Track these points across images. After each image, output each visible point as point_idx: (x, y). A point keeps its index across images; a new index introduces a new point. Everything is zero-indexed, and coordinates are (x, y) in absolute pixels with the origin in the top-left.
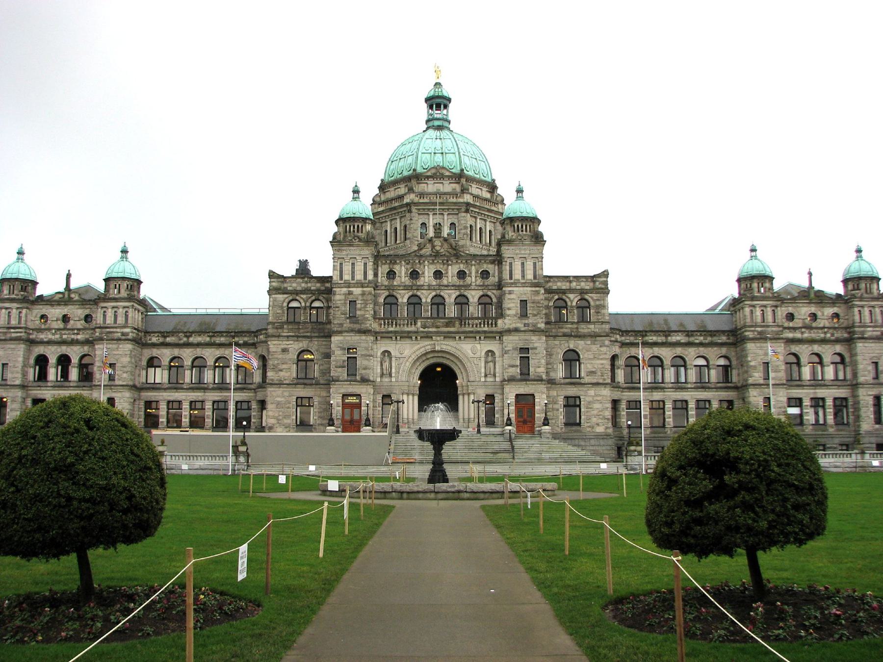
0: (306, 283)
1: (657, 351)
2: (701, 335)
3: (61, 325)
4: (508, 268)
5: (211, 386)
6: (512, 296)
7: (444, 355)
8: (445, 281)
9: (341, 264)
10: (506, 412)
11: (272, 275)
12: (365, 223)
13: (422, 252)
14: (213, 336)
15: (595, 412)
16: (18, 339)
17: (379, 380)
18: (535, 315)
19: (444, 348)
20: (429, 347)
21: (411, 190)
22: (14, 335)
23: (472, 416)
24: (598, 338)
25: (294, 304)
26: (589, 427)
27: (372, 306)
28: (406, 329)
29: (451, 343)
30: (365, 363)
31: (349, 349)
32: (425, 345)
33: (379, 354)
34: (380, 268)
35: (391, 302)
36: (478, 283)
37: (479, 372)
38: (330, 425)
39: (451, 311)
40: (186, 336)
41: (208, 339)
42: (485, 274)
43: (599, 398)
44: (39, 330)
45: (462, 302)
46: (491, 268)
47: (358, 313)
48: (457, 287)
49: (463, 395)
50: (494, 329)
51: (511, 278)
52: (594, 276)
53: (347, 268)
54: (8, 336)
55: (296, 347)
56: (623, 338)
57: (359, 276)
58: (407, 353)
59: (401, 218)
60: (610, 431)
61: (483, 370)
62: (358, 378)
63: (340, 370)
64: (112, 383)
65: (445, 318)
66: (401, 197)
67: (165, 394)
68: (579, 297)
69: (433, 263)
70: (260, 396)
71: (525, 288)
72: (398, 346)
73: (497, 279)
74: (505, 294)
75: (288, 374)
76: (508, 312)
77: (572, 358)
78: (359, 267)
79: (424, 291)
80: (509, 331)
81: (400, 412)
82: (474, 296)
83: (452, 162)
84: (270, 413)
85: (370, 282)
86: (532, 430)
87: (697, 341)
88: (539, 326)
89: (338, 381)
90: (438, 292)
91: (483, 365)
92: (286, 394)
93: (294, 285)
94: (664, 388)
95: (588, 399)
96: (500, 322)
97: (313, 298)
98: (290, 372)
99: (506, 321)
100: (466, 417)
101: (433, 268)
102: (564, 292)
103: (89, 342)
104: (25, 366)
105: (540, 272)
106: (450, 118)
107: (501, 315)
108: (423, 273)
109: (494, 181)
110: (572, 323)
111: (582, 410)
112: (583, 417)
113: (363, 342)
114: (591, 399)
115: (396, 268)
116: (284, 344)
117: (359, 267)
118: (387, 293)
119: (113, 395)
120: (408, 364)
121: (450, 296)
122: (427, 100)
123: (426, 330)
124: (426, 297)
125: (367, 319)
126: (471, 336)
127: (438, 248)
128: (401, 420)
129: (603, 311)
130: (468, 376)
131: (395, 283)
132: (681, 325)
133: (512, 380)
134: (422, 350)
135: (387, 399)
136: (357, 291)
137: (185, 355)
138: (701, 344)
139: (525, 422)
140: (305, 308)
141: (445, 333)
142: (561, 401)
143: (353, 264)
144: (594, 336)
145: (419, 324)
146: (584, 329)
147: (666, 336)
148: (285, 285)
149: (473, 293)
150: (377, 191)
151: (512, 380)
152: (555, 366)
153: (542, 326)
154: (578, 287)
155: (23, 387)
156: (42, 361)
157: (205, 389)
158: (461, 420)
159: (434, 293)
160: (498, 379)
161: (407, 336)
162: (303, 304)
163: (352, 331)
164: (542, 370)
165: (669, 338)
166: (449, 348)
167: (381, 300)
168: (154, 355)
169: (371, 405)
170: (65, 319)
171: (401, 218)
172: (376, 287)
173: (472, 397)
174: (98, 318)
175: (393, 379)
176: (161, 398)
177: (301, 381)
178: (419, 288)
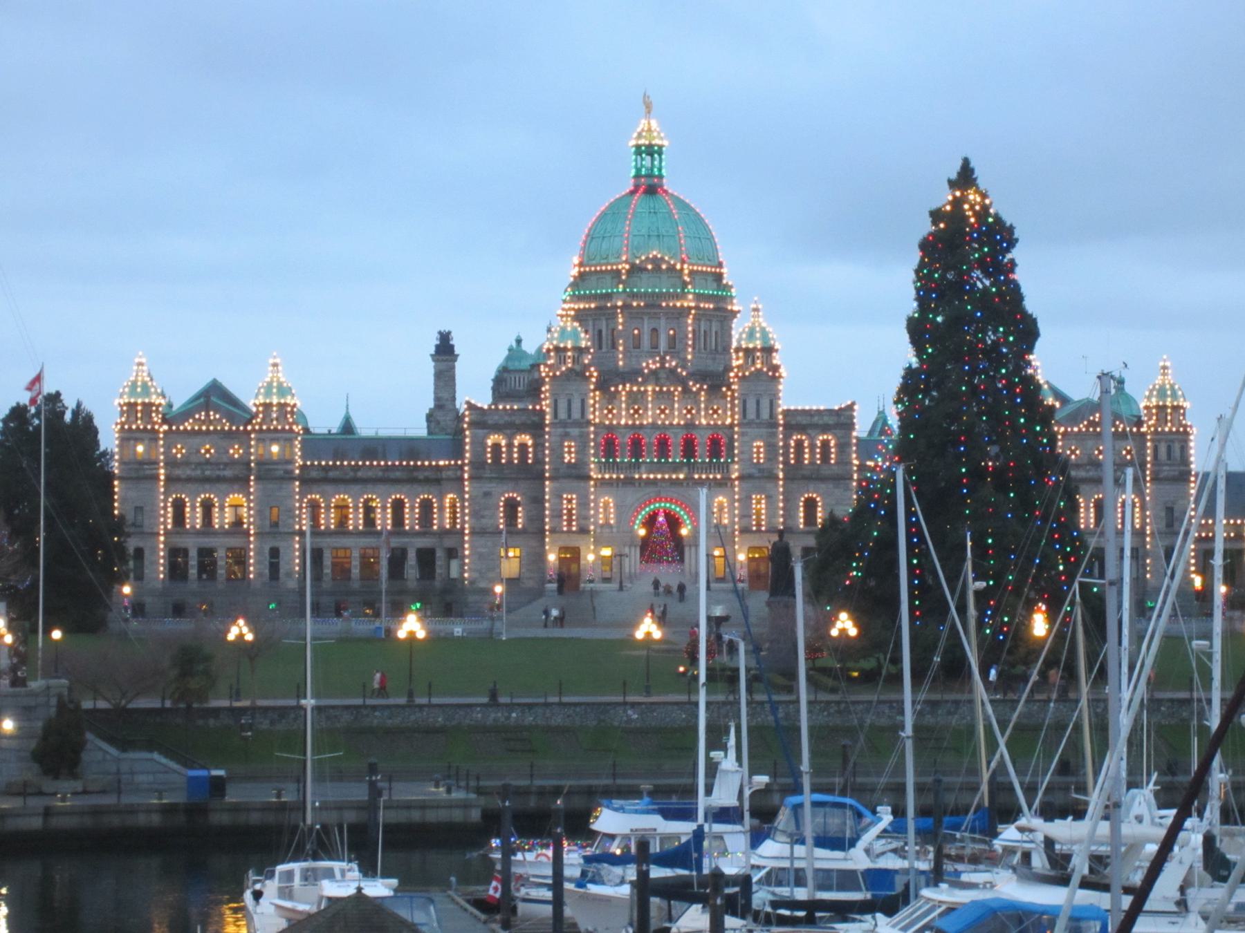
6: (746, 439)
10: (738, 566)
22: (148, 472)
52: (841, 409)
53: (563, 406)
54: (141, 473)
57: (576, 415)
64: (275, 530)
70: (449, 542)
78: (576, 406)
92: (489, 544)
93: (496, 417)
108: (646, 409)
116: (487, 486)
117: (576, 406)
119: (276, 544)
133: (745, 530)
136: (575, 431)
141: (670, 479)
145: (643, 468)
160: (729, 530)
161: (629, 482)
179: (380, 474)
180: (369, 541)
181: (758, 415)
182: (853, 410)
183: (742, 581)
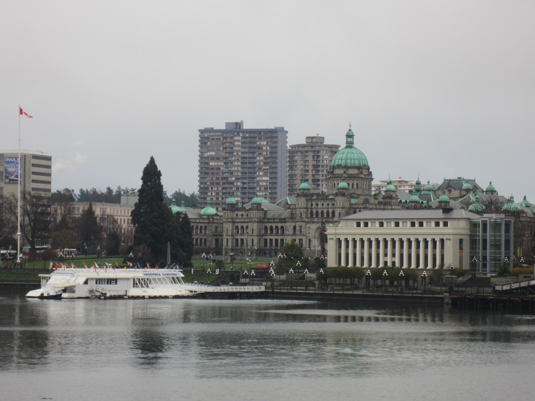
3: (241, 217)
16: (230, 222)
35: (312, 213)
39: (325, 216)
42: (334, 205)
44: (236, 219)
45: (328, 212)
53: (300, 204)
82: (330, 211)
98: (291, 232)
103: (247, 222)
104: (232, 229)
113: (303, 224)
121: (325, 211)
122: (347, 136)
124: (320, 211)
135: (310, 240)
136: (302, 210)
155: (232, 235)
156: (237, 227)
157: (278, 235)
161: (313, 222)
167: (309, 212)
170: (242, 215)
174: (249, 216)
178: (318, 208)
180: (276, 237)
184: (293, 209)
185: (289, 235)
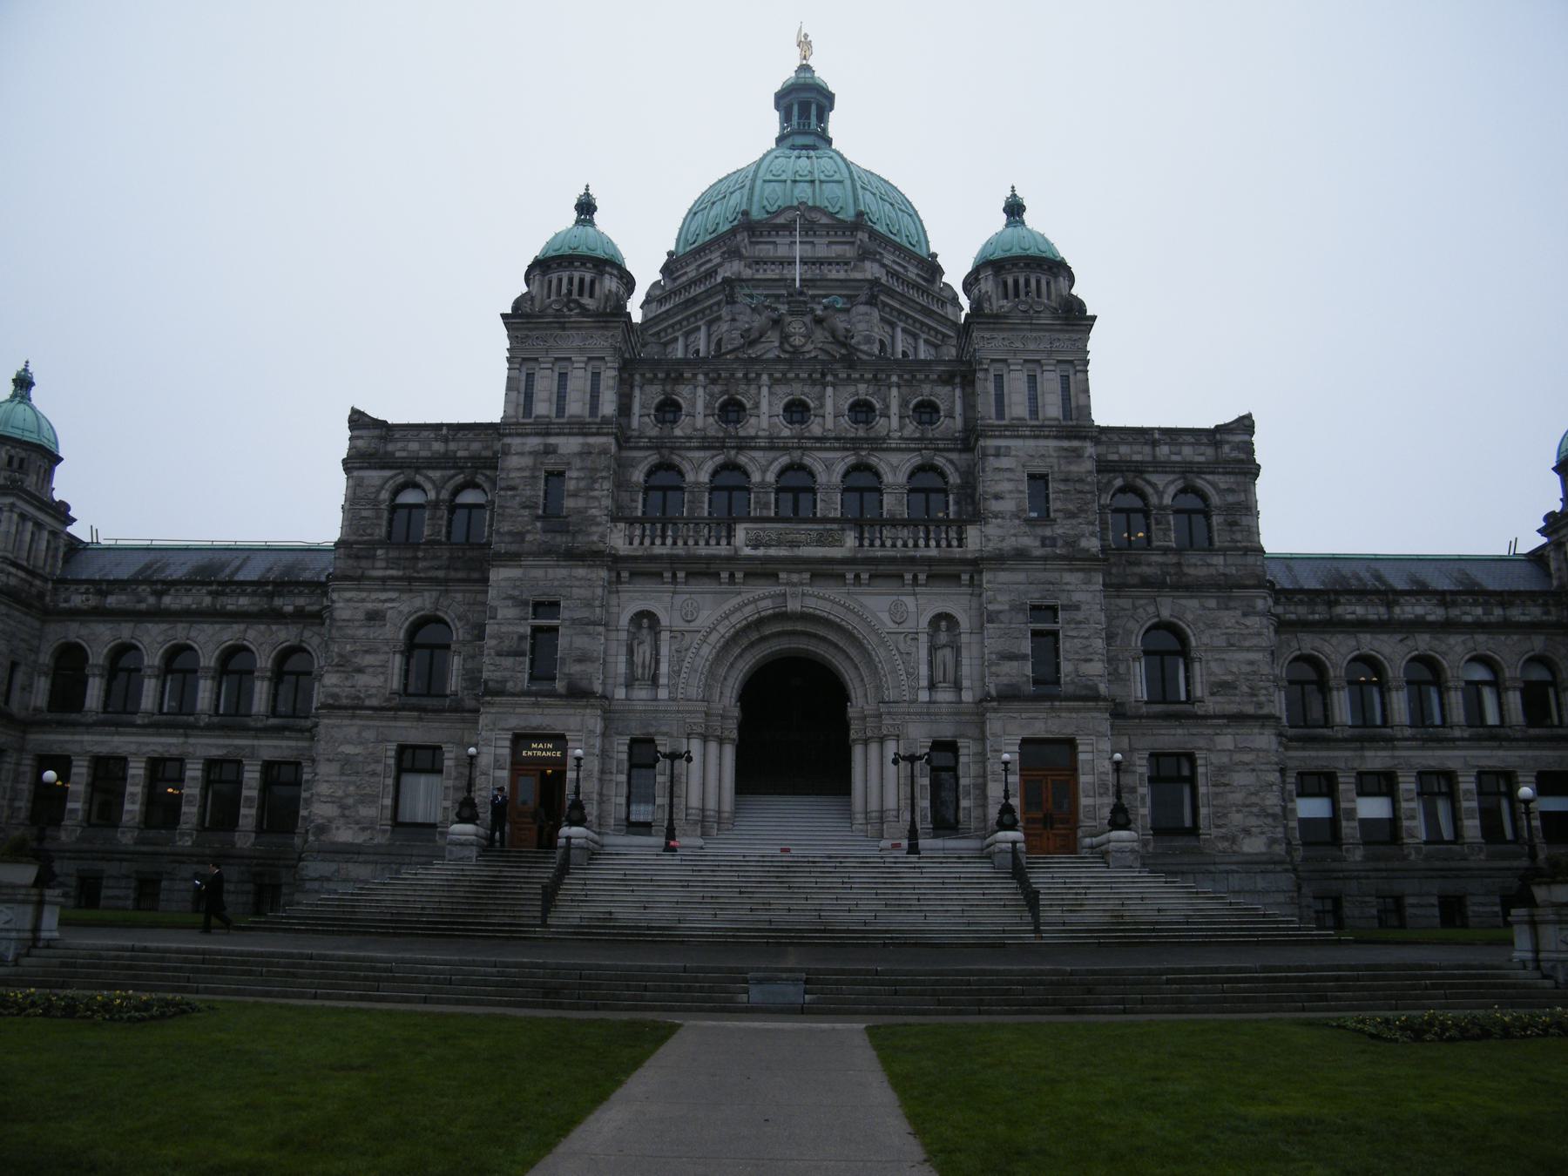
0: (446, 440)
1: (1370, 643)
2: (1475, 604)
4: (991, 387)
5: (205, 720)
6: (1005, 462)
7: (811, 629)
8: (816, 429)
9: (530, 377)
10: (995, 791)
11: (358, 421)
12: (602, 273)
13: (753, 352)
14: (223, 594)
15: (1238, 797)
17: (620, 693)
18: (1071, 515)
19: (814, 605)
20: (768, 603)
21: (735, 254)
23: (891, 803)
24: (1236, 593)
25: (410, 497)
26: (1224, 838)
27: (607, 485)
28: (703, 550)
29: (832, 591)
30: (581, 642)
31: (537, 605)
32: (757, 599)
33: (624, 620)
34: (637, 392)
36: (906, 433)
37: (912, 675)
38: (462, 820)
39: (830, 504)
40: (154, 593)
41: (207, 600)
42: (927, 410)
43: (1247, 758)
45: (862, 482)
46: (949, 398)
47: (569, 503)
48: (852, 444)
49: (866, 742)
50: (957, 552)
51: (1000, 414)
52: (1219, 429)
53: (545, 385)
55: (405, 608)
56: (1279, 610)
58: (705, 618)
59: (710, 324)
60: (1280, 849)
61: (924, 670)
62: (560, 686)
63: (508, 662)
65: (815, 520)
66: (712, 273)
67: (86, 738)
68: (1180, 484)
69: (784, 380)
71: (1042, 442)
72: (679, 599)
73: (959, 423)
74: (985, 455)
75: (378, 681)
76: (995, 506)
77: (1169, 647)
78: (579, 382)
79: (757, 454)
80: (999, 560)
81: (680, 790)
82: (895, 469)
83: (835, 198)
84: (323, 789)
85: (606, 421)
86: (1069, 846)
87: (1468, 619)
88: (1084, 543)
89: (501, 693)
90: (797, 454)
91: (923, 653)
92: (369, 735)
93: (414, 446)
94: (1392, 739)
95: (1215, 759)
96: (972, 534)
97: (460, 478)
98: (383, 674)
99: (992, 529)
100: (874, 805)
101: (784, 395)
102: (1139, 469)
105: (1082, 397)
106: (832, 132)
107: (973, 511)
108: (757, 406)
109: (935, 256)
110: (1166, 551)
111: (1202, 790)
112: (1203, 811)
113: (578, 585)
114: (1225, 760)
115: (683, 394)
116: (375, 600)
117: (579, 382)
118: (653, 458)
120: (705, 650)
121: (829, 469)
123: (761, 552)
124: (763, 469)
125: (593, 521)
126: (886, 572)
127: (797, 341)
128: (680, 815)
129: (1245, 521)
130: (879, 688)
131: (678, 432)
132: (1417, 582)
133: (1009, 696)
134: (748, 610)
136: (569, 445)
137: (146, 640)
138: (1479, 626)
139: (1048, 821)
140: (435, 505)
142: (1142, 767)
143: (563, 377)
144: (1225, 587)
145: (741, 532)
146: (1198, 567)
147: (1389, 606)
148: (390, 447)
149: (894, 458)
150: (659, 277)
151: (1009, 696)
152: (1122, 669)
153: (1093, 544)
154: (1175, 458)
157: (189, 729)
158: (859, 818)
159: (785, 460)
160: (967, 696)
161: (703, 570)
162: (432, 495)
163: (546, 552)
164: (1096, 668)
165: (1397, 610)
166: (828, 606)
167: (638, 476)
168: (72, 638)
169: (593, 765)
171: (710, 324)
172: (624, 440)
173: (891, 748)
175: (663, 694)
176: (76, 748)
177: (414, 700)
178: (744, 445)
179: (207, 600)
181: (1034, 412)
182: (1252, 433)
183: (1012, 828)
184: (416, 465)
185: (354, 707)
